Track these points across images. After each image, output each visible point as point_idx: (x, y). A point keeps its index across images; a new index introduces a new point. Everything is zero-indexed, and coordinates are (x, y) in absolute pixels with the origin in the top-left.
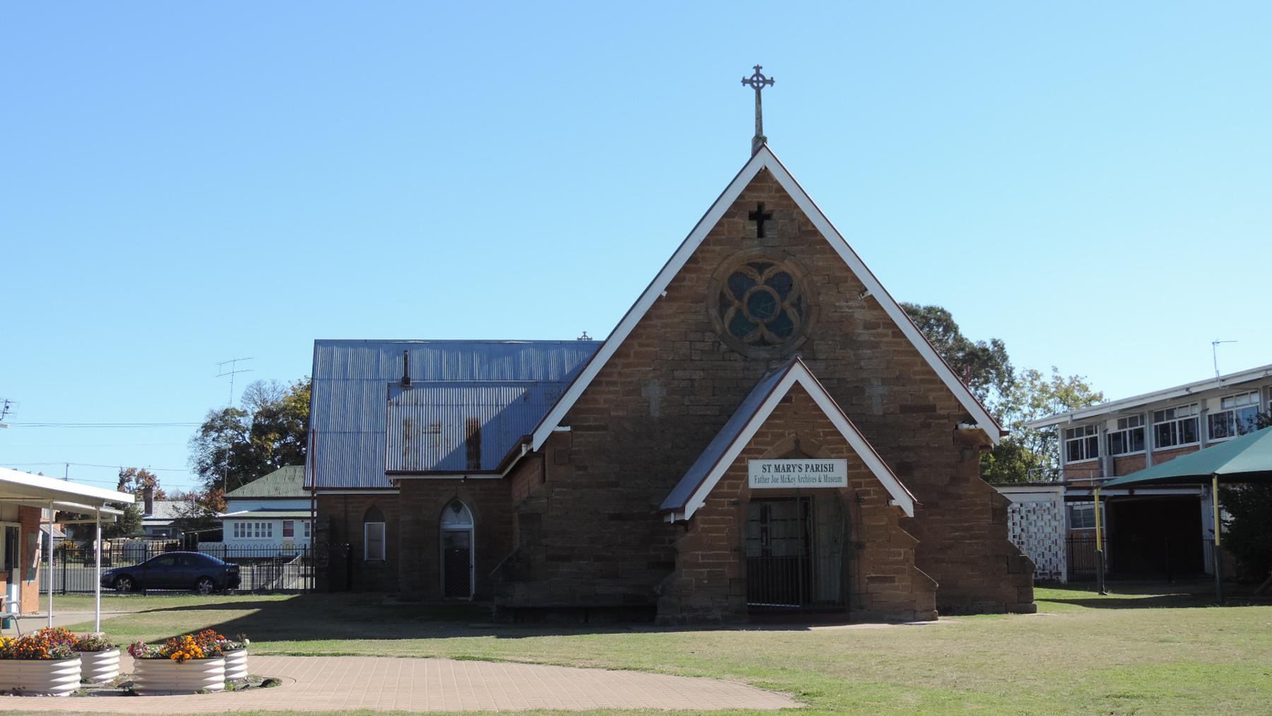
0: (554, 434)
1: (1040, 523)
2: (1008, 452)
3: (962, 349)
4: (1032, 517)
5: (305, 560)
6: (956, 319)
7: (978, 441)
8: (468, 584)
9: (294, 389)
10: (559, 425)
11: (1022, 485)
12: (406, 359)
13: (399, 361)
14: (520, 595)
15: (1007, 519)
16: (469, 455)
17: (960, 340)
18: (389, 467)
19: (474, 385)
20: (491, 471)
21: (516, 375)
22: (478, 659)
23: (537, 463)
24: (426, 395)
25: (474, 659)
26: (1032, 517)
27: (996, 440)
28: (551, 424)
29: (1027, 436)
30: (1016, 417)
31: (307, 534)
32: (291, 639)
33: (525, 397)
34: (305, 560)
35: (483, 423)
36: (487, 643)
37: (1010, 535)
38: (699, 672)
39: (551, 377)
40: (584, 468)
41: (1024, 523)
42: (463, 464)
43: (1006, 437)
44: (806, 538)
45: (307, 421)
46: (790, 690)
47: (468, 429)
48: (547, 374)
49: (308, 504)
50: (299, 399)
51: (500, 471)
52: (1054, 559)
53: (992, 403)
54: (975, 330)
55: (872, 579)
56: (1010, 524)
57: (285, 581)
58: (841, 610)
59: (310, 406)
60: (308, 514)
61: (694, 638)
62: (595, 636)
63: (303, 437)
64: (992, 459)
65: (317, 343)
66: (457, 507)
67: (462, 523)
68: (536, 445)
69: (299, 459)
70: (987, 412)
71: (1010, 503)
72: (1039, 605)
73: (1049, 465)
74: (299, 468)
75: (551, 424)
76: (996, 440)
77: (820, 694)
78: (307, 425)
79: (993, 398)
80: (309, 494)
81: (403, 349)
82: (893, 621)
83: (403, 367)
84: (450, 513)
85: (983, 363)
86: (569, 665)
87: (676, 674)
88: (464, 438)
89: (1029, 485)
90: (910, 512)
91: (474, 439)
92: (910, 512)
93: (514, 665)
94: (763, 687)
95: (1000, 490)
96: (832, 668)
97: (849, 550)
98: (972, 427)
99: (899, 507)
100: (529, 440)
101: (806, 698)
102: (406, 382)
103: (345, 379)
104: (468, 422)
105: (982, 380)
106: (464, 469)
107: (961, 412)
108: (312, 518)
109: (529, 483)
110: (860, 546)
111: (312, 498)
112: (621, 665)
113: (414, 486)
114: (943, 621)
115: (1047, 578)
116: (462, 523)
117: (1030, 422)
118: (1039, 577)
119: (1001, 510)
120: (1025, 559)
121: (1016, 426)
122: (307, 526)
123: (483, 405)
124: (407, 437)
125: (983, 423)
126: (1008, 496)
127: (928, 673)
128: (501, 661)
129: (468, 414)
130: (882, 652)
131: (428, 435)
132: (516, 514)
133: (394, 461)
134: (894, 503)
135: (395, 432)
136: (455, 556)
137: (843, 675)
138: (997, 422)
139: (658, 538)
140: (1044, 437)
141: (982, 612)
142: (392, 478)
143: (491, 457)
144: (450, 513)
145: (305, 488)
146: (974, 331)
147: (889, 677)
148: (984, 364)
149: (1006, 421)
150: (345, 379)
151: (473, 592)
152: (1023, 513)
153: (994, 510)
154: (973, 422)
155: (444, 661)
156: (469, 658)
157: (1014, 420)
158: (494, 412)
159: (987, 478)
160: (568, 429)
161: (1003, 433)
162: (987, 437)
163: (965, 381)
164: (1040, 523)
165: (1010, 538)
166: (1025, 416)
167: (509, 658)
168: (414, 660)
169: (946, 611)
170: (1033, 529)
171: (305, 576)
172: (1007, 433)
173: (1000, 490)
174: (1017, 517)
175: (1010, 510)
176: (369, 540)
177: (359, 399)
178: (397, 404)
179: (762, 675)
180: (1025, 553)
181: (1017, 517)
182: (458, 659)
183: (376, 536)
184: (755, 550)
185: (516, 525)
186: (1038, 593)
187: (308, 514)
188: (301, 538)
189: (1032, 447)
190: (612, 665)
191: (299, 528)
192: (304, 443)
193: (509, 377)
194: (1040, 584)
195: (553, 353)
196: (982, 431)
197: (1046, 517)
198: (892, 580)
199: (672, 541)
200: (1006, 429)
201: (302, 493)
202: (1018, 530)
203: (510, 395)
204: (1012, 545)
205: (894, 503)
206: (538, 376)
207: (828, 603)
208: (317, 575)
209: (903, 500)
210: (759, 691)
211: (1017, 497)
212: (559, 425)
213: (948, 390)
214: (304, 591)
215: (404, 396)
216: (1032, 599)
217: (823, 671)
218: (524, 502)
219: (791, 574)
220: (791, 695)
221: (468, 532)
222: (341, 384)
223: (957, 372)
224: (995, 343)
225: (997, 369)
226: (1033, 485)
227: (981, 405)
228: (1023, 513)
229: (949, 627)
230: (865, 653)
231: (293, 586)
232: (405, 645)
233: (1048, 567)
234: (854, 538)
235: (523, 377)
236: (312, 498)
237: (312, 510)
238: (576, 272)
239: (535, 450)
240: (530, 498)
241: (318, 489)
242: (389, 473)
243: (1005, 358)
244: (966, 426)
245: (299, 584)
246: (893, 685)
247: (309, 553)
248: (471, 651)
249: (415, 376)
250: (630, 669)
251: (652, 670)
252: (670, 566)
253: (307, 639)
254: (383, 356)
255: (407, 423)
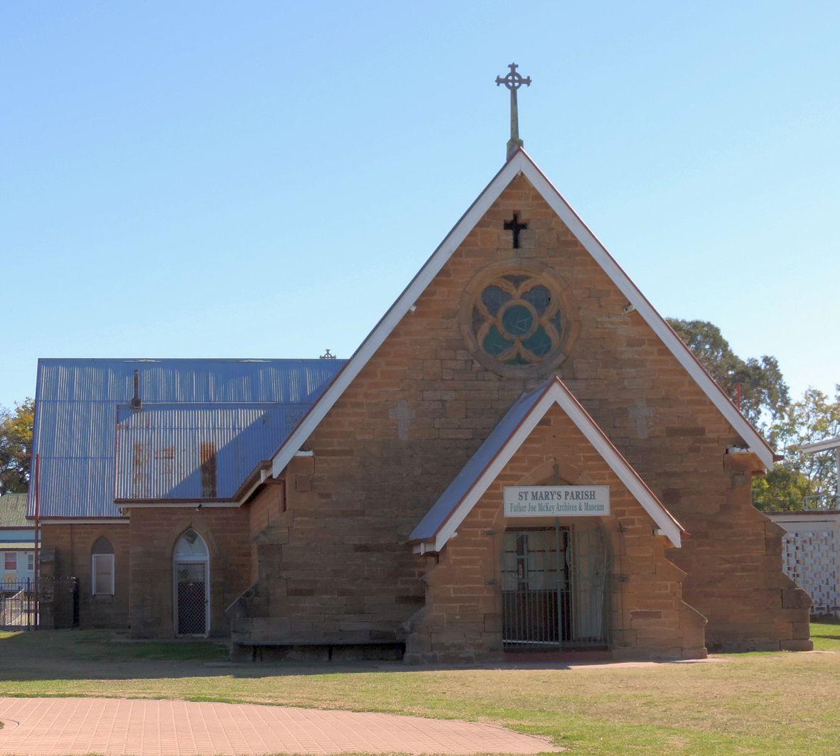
0: (294, 461)
1: (817, 554)
2: (782, 478)
3: (733, 367)
4: (809, 548)
5: (28, 594)
6: (725, 335)
7: (750, 467)
8: (203, 617)
9: (18, 411)
10: (302, 449)
11: (797, 513)
12: (136, 379)
13: (129, 381)
14: (259, 632)
15: (781, 550)
16: (204, 483)
17: (732, 361)
18: (119, 494)
19: (210, 407)
20: (232, 495)
21: (254, 398)
22: (214, 701)
23: (275, 492)
24: (158, 417)
25: (210, 700)
26: (809, 548)
27: (769, 466)
28: (291, 450)
29: (802, 462)
30: (792, 440)
31: (30, 567)
32: (14, 679)
33: (264, 420)
34: (28, 594)
35: (219, 447)
36: (225, 683)
37: (785, 567)
38: (451, 714)
39: (292, 399)
40: (328, 496)
41: (800, 554)
42: (197, 491)
43: (781, 462)
44: (566, 570)
45: (30, 445)
46: (548, 734)
47: (204, 454)
48: (287, 395)
49: (32, 534)
50: (20, 422)
51: (238, 500)
52: (832, 592)
53: (764, 425)
54: (746, 347)
55: (636, 614)
56: (784, 555)
57: (8, 617)
58: (602, 648)
59: (33, 430)
60: (32, 545)
61: (445, 677)
62: (340, 676)
63: (26, 463)
64: (766, 486)
65: (41, 362)
66: (192, 537)
67: (197, 554)
68: (276, 471)
69: (22, 487)
70: (760, 435)
71: (782, 532)
72: (817, 643)
73: (826, 492)
74: (22, 496)
75: (291, 450)
76: (769, 466)
77: (581, 737)
78: (30, 450)
79: (766, 419)
80: (33, 525)
81: (133, 369)
82: (658, 659)
83: (132, 388)
84: (183, 542)
85: (758, 382)
86: (312, 707)
87: (426, 716)
88: (199, 463)
89: (804, 513)
90: (677, 542)
91: (209, 467)
92: (677, 542)
93: (252, 707)
94: (521, 730)
95: (774, 519)
96: (593, 709)
97: (611, 583)
98: (744, 451)
99: (666, 538)
100: (268, 466)
101: (566, 742)
102: (136, 403)
103: (71, 401)
104: (203, 446)
105: (753, 400)
106: (199, 497)
107: (732, 436)
108: (36, 550)
109: (268, 511)
110: (623, 579)
111: (37, 529)
112: (367, 706)
113: (144, 514)
114: (713, 660)
115: (824, 612)
116: (197, 554)
117: (808, 446)
118: (817, 612)
119: (774, 542)
120: (800, 593)
121: (792, 450)
122: (30, 557)
123: (220, 428)
124: (137, 462)
125: (756, 447)
126: (783, 526)
127: (696, 715)
128: (239, 702)
129: (201, 438)
130: (648, 693)
131: (164, 461)
132: (254, 546)
133: (123, 488)
134: (660, 533)
135: (123, 458)
136: (190, 597)
137: (605, 717)
138: (771, 446)
139: (408, 571)
140: (822, 461)
141: (754, 650)
142: (123, 506)
143: (228, 484)
144: (183, 542)
145: (29, 518)
146: (745, 349)
147: (655, 719)
148: (756, 383)
149: (780, 444)
150: (71, 401)
151: (208, 628)
152: (799, 544)
153: (767, 541)
154: (745, 445)
155: (177, 703)
156: (205, 700)
157: (790, 444)
158: (231, 436)
159: (758, 506)
160: (310, 453)
161: (777, 458)
162: (760, 462)
163: (736, 403)
164: (817, 554)
165: (785, 571)
166: (802, 439)
167: (248, 699)
168: (145, 702)
169: (716, 648)
170: (809, 561)
171: (29, 612)
172: (781, 458)
173: (774, 519)
174: (792, 548)
175: (784, 541)
176: (98, 574)
177: (86, 421)
178: (127, 428)
179: (518, 716)
180: (800, 586)
181: (792, 548)
182: (192, 700)
183: (103, 572)
184: (511, 584)
185: (255, 558)
186: (815, 629)
187: (32, 545)
188: (24, 572)
189: (809, 473)
190: (358, 706)
191: (22, 561)
192: (27, 468)
193: (247, 398)
194: (815, 619)
195: (294, 373)
196: (754, 455)
197: (824, 548)
198: (657, 615)
199: (422, 574)
200: (780, 453)
201: (25, 523)
202: (793, 562)
203: (247, 418)
204: (786, 578)
205: (660, 533)
206: (279, 398)
207: (590, 640)
208: (41, 610)
209: (670, 529)
210: (516, 734)
211: (790, 526)
212: (302, 449)
213: (718, 412)
214: (28, 628)
215: (134, 419)
216: (808, 635)
217: (584, 713)
218: (264, 533)
219: (548, 614)
220: (548, 738)
221: (203, 564)
222: (68, 406)
223: (727, 392)
224: (766, 360)
225: (769, 389)
226: (809, 513)
227: (753, 428)
228: (799, 544)
229: (719, 665)
230: (628, 693)
231: (16, 622)
232: (135, 685)
233: (826, 601)
234: (616, 570)
235: (263, 398)
236: (37, 529)
237: (36, 541)
238: (314, 286)
239: (275, 477)
240: (270, 528)
241: (42, 518)
242: (118, 501)
243: (779, 377)
244: (737, 450)
245: (22, 620)
246: (659, 728)
247: (32, 587)
248: (206, 692)
249: (146, 397)
250: (376, 711)
251: (401, 712)
252: (419, 600)
253: (31, 678)
254: (111, 377)
255: (137, 448)
